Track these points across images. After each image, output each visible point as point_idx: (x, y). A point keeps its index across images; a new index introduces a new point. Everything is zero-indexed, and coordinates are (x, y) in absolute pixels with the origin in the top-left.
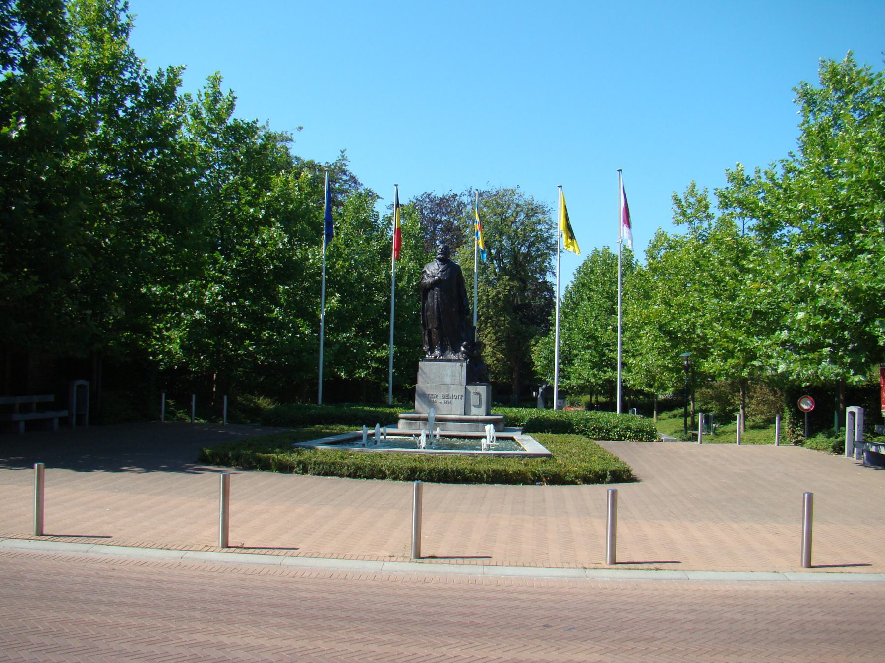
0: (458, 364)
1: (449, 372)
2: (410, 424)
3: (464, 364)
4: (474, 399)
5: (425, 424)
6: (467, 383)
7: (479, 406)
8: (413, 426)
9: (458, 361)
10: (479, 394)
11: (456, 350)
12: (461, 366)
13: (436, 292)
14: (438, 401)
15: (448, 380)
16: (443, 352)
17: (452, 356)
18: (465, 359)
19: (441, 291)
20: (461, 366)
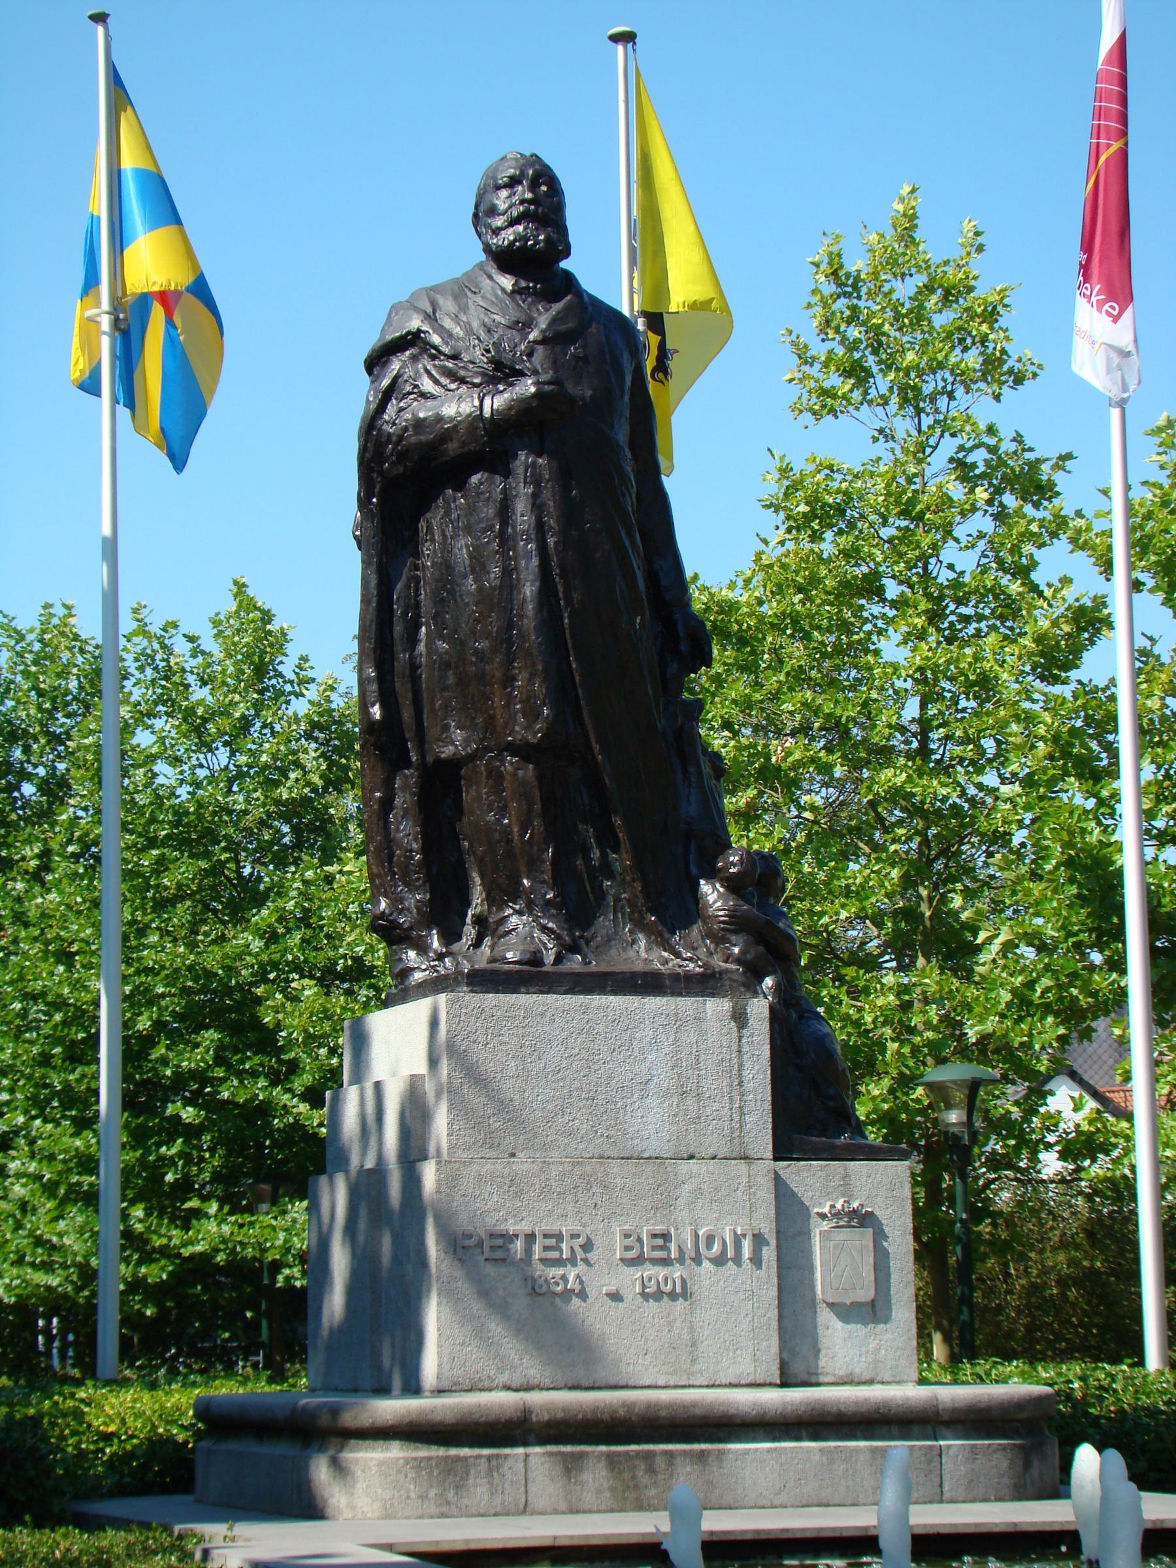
0: (717, 1007)
1: (657, 1063)
2: (455, 1474)
3: (759, 1008)
4: (835, 1264)
5: (571, 1467)
6: (782, 1151)
7: (872, 1311)
8: (479, 1491)
9: (704, 984)
10: (862, 1219)
11: (673, 911)
12: (740, 1018)
13: (523, 490)
14: (600, 1282)
15: (652, 1124)
16: (577, 913)
17: (643, 954)
18: (754, 973)
19: (565, 475)
20: (740, 1018)
